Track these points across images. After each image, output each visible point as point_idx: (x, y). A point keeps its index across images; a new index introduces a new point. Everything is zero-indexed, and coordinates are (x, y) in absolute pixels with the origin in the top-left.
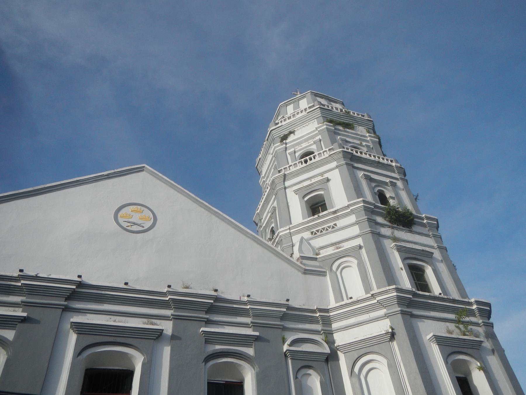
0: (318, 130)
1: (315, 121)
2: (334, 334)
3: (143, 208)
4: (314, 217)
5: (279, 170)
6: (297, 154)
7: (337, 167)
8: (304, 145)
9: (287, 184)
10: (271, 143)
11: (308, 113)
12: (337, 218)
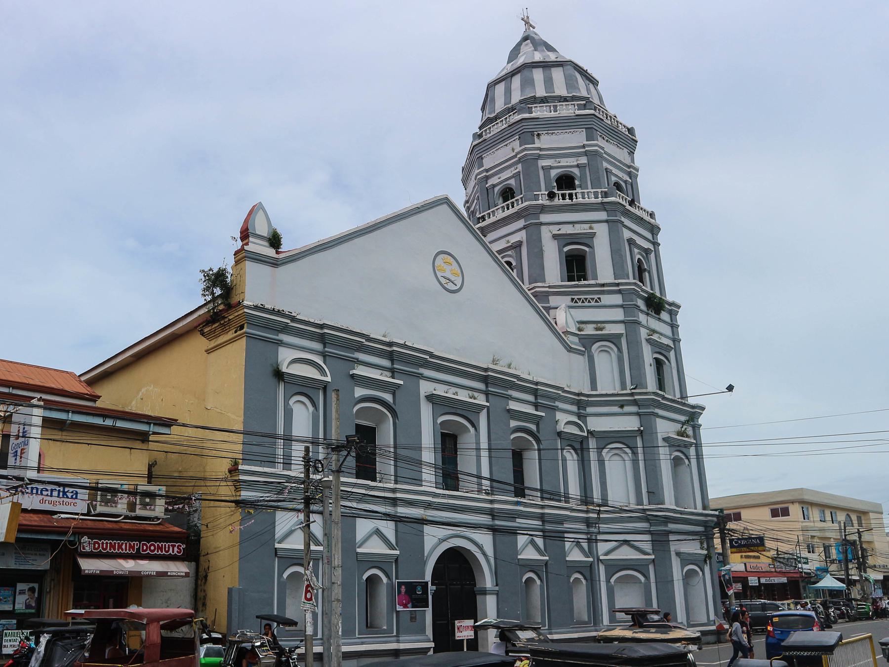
0: (587, 149)
1: (583, 131)
2: (587, 418)
3: (452, 260)
4: (579, 284)
5: (535, 193)
6: (554, 173)
7: (607, 221)
8: (564, 162)
9: (545, 218)
10: (517, 133)
11: (577, 115)
12: (603, 292)
